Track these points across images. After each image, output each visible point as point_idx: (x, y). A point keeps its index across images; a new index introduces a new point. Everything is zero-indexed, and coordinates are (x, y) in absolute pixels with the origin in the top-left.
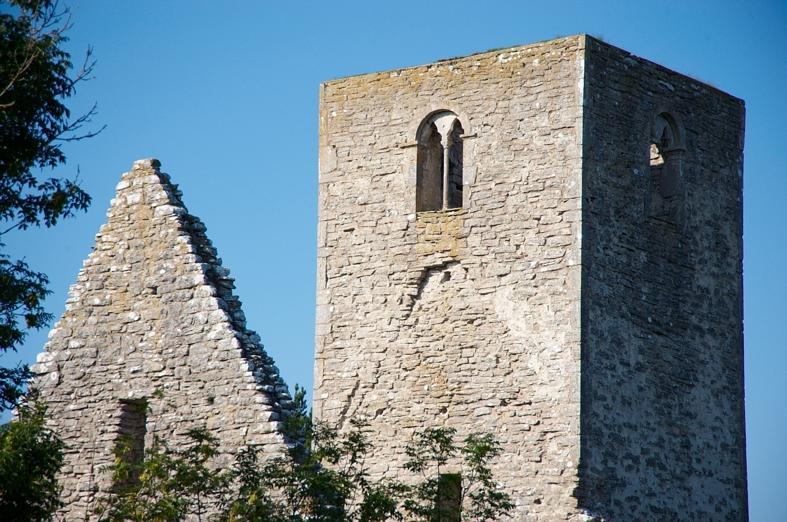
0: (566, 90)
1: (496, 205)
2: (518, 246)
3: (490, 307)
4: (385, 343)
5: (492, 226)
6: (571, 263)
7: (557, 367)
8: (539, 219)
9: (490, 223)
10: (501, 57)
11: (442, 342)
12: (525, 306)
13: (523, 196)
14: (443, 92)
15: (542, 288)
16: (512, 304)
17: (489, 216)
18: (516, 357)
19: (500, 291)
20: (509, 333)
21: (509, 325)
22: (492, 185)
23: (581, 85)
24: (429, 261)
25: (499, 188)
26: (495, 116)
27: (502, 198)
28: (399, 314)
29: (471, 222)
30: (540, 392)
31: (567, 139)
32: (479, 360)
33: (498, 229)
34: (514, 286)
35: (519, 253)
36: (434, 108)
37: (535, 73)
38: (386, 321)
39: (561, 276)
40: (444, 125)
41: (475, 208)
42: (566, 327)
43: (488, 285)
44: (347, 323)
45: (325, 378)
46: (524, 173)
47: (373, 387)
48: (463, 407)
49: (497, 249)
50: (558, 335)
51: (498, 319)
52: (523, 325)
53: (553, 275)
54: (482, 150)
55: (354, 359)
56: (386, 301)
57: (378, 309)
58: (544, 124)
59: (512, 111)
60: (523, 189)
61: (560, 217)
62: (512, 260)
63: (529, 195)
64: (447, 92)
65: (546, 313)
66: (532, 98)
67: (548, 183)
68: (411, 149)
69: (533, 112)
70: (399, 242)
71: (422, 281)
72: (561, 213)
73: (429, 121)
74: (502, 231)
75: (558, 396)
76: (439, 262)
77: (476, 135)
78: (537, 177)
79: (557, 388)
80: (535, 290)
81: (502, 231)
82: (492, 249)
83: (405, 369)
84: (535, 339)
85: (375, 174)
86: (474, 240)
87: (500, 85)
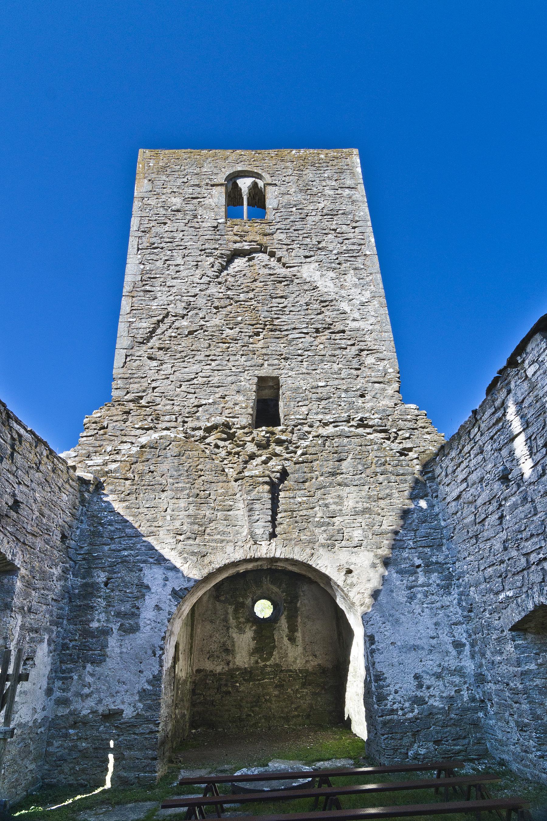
0: (348, 171)
1: (298, 220)
2: (319, 242)
3: (298, 274)
4: (193, 291)
5: (295, 230)
6: (368, 253)
7: (367, 310)
8: (335, 230)
9: (294, 228)
10: (294, 152)
12: (332, 274)
13: (320, 218)
14: (246, 163)
15: (344, 265)
16: (318, 273)
17: (291, 224)
18: (327, 303)
19: (305, 267)
20: (319, 289)
22: (294, 209)
23: (359, 170)
24: (237, 246)
25: (300, 211)
26: (291, 177)
27: (302, 216)
28: (211, 274)
29: (277, 227)
31: (352, 192)
33: (300, 232)
34: (319, 263)
35: (320, 246)
36: (240, 169)
37: (321, 161)
39: (360, 260)
41: (278, 220)
42: (370, 288)
43: (294, 261)
44: (158, 276)
45: (133, 308)
46: (321, 206)
47: (183, 318)
49: (301, 243)
50: (364, 292)
51: (307, 281)
52: (330, 284)
53: (352, 259)
54: (282, 192)
55: (163, 298)
56: (197, 265)
57: (189, 269)
58: (332, 184)
59: (305, 177)
60: (320, 214)
61: (353, 230)
62: (314, 249)
63: (325, 217)
65: (351, 278)
66: (322, 172)
68: (219, 188)
69: (323, 178)
70: (210, 233)
71: (230, 260)
72: (354, 228)
73: (233, 178)
74: (304, 233)
75: (371, 328)
77: (275, 185)
78: (331, 208)
79: (370, 322)
80: (338, 266)
81: (304, 233)
82: (296, 242)
84: (343, 293)
85: (187, 197)
87: (295, 163)
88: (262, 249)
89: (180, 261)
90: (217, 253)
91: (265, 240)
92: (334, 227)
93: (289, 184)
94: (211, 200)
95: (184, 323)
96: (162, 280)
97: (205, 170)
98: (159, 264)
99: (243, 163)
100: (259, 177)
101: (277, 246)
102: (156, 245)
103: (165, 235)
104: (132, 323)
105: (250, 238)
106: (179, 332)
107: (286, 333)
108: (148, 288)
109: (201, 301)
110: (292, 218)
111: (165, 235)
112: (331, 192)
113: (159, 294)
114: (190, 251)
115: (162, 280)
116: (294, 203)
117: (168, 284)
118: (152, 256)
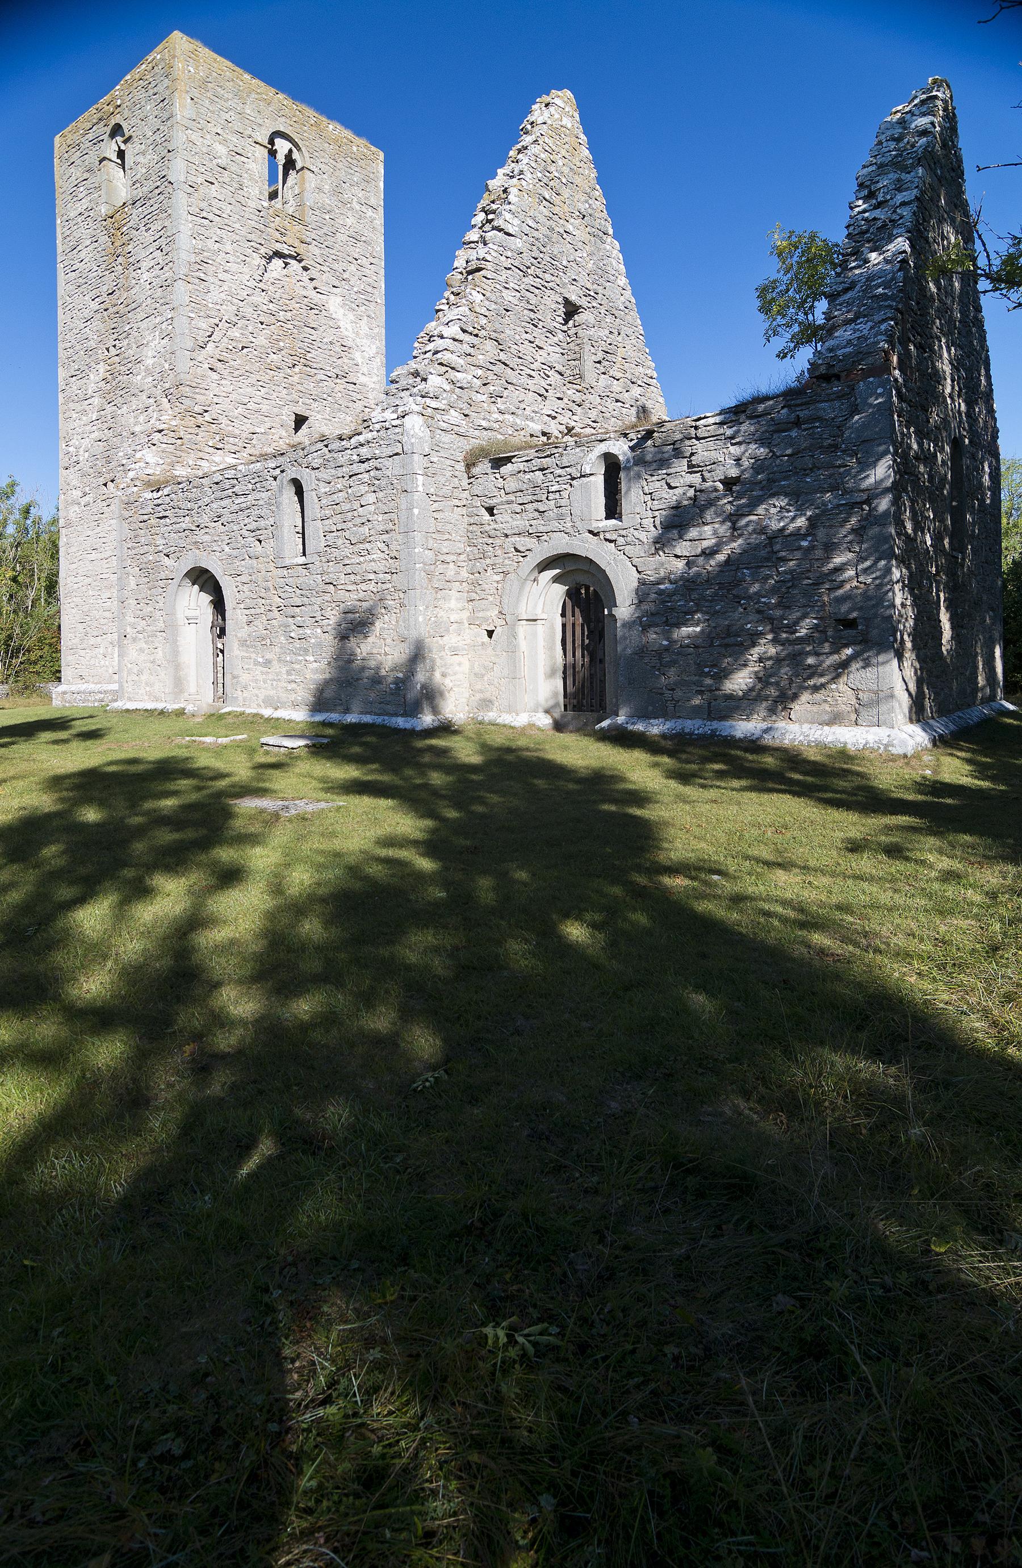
9: (326, 243)
10: (331, 127)
11: (289, 314)
19: (332, 297)
21: (341, 324)
22: (327, 217)
24: (278, 247)
30: (363, 379)
32: (318, 340)
36: (282, 129)
38: (248, 277)
40: (282, 146)
48: (308, 369)
55: (215, 295)
57: (238, 263)
64: (292, 123)
67: (364, 238)
76: (286, 252)
79: (373, 380)
83: (262, 323)
86: (313, 249)
88: (297, 258)
89: (228, 248)
90: (263, 251)
91: (301, 249)
92: (356, 256)
93: (325, 176)
94: (254, 165)
95: (235, 333)
96: (214, 268)
97: (248, 112)
98: (210, 243)
99: (283, 119)
100: (299, 149)
101: (312, 263)
102: (204, 214)
103: (214, 202)
104: (192, 319)
105: (290, 242)
106: (234, 345)
107: (316, 371)
108: (202, 276)
109: (248, 311)
110: (325, 230)
111: (214, 202)
112: (358, 207)
113: (212, 288)
114: (238, 238)
115: (214, 268)
116: (328, 208)
117: (220, 276)
118: (202, 230)
